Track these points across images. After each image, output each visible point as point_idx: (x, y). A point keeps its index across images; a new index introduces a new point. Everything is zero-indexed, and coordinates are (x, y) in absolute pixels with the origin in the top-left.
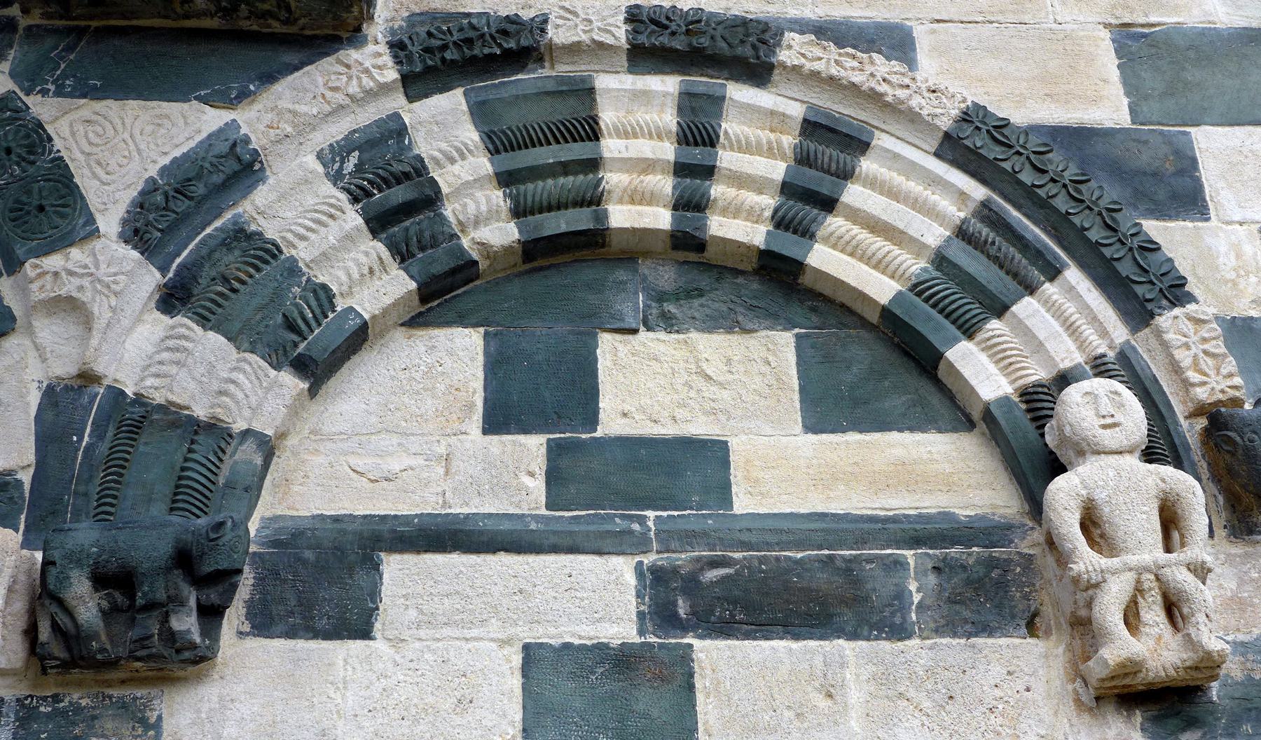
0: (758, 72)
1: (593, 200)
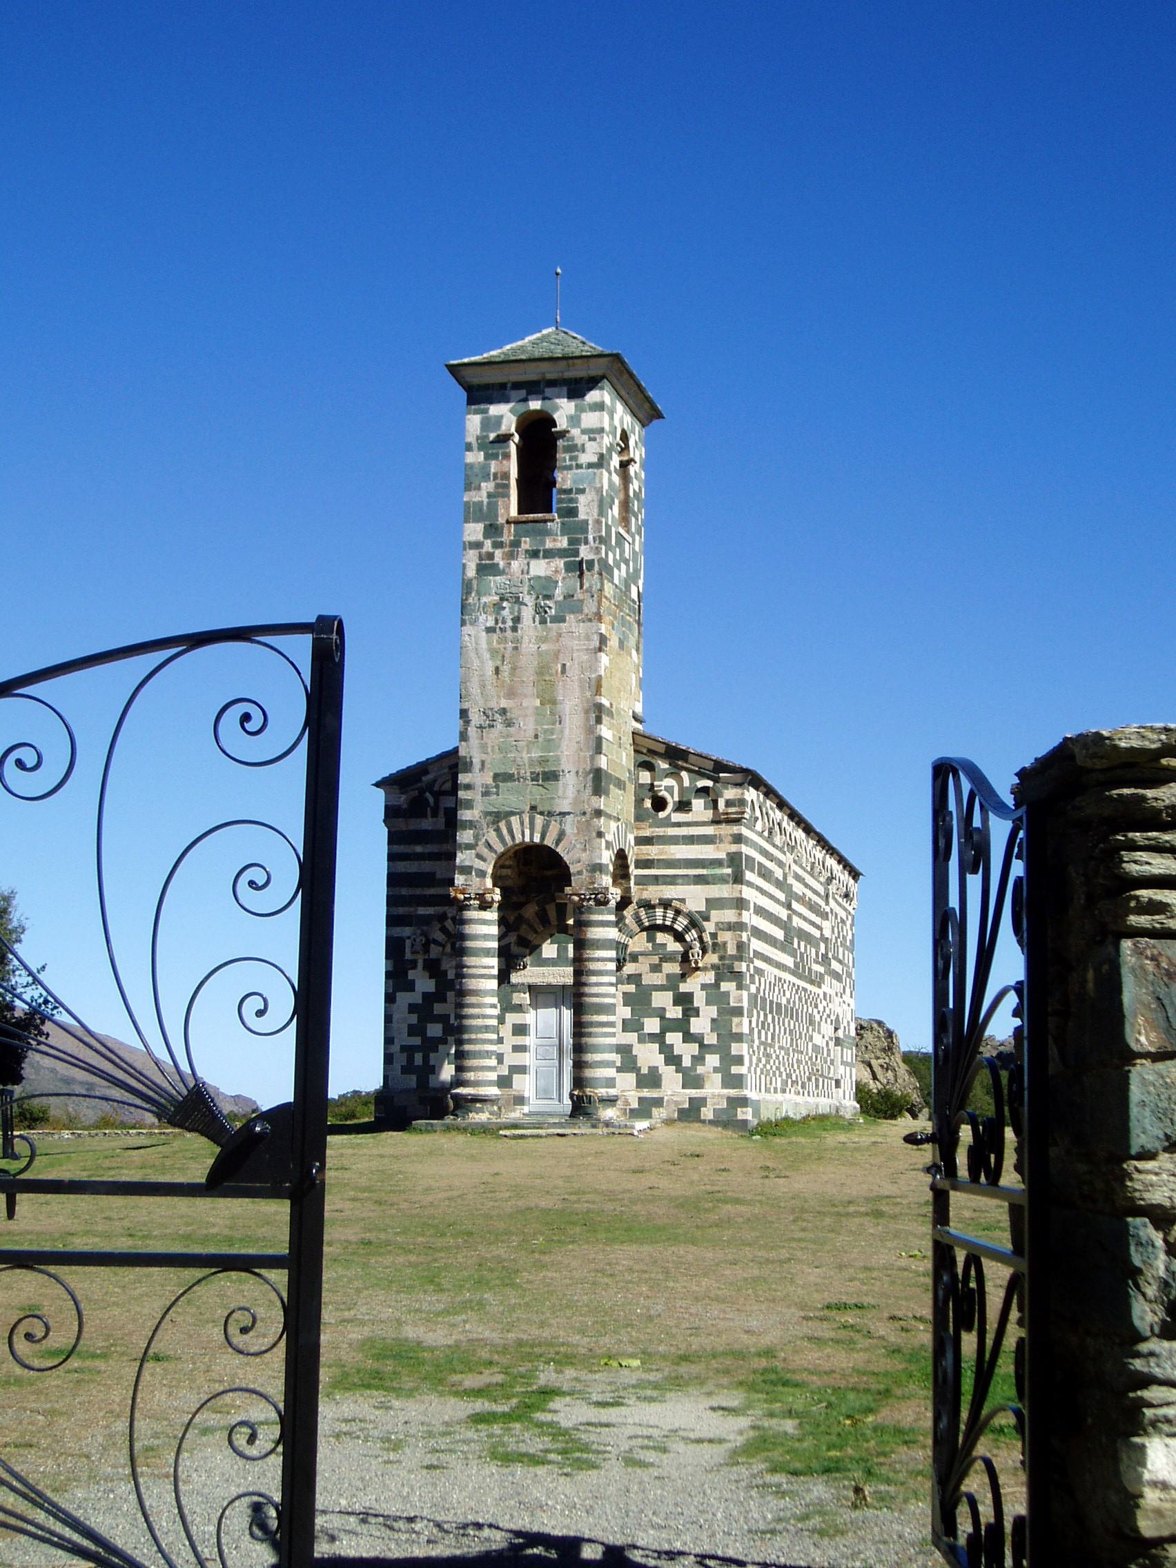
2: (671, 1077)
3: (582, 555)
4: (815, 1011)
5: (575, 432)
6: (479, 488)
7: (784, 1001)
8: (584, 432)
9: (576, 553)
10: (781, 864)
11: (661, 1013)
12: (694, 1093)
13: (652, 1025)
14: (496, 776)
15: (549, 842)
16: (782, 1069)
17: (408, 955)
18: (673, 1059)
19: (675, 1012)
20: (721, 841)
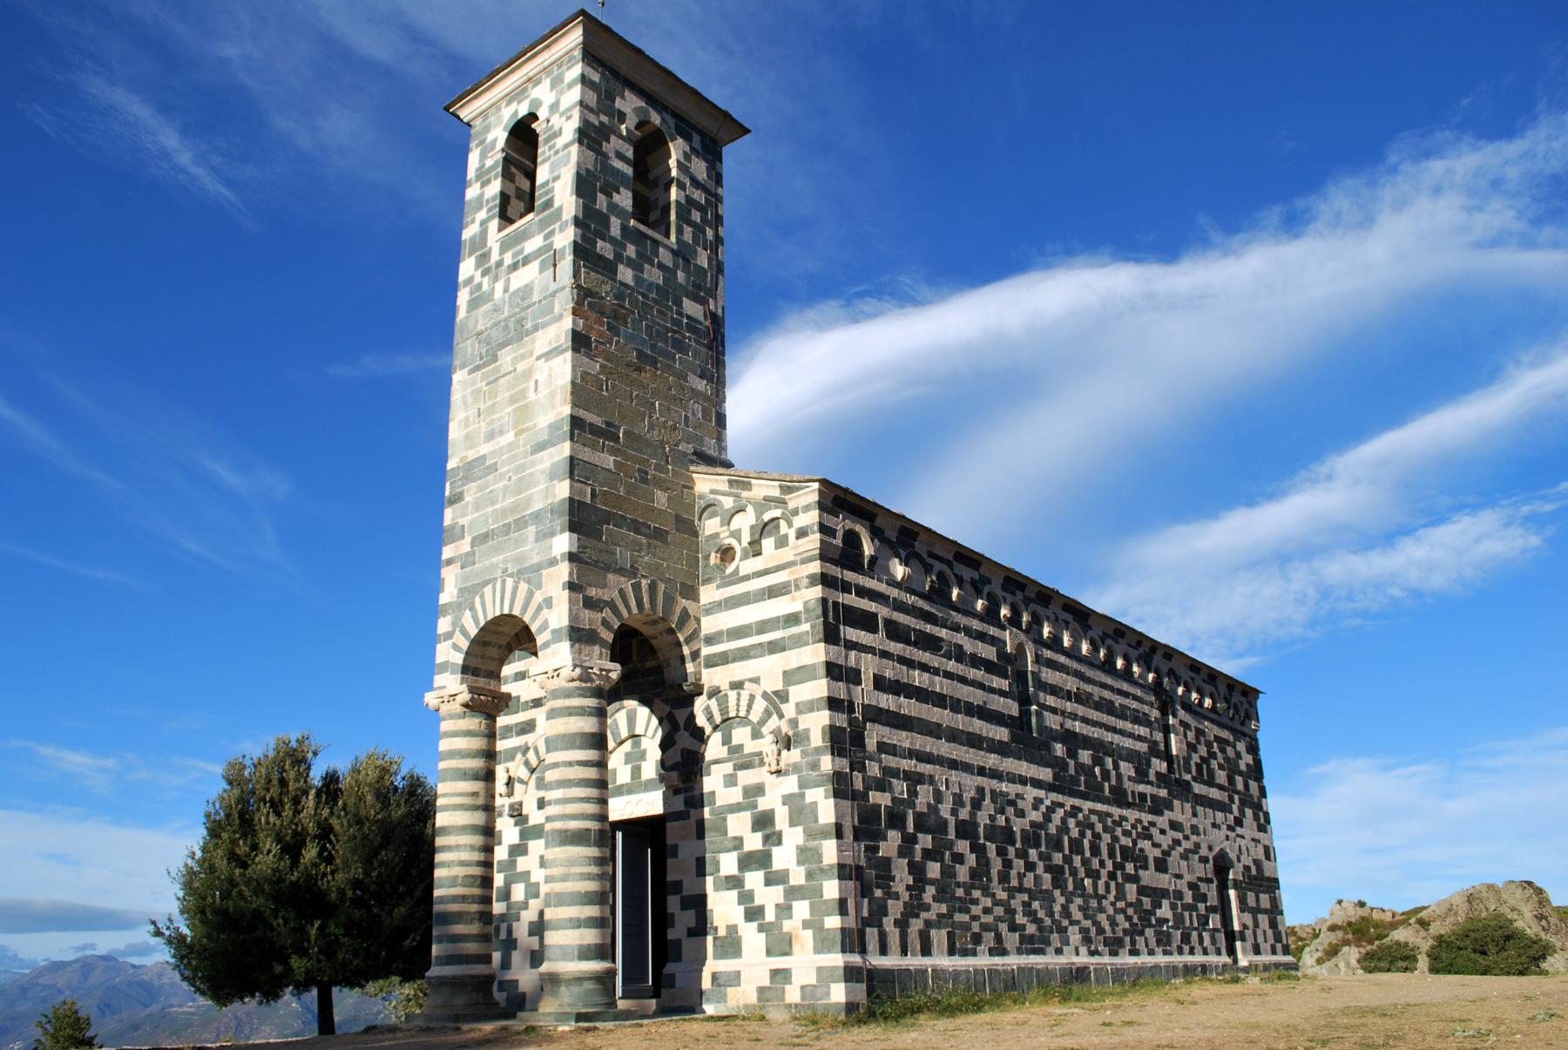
4: (1145, 844)
7: (1018, 825)
10: (982, 637)
11: (738, 843)
12: (780, 962)
16: (1020, 919)
18: (754, 913)
19: (754, 842)
20: (797, 588)
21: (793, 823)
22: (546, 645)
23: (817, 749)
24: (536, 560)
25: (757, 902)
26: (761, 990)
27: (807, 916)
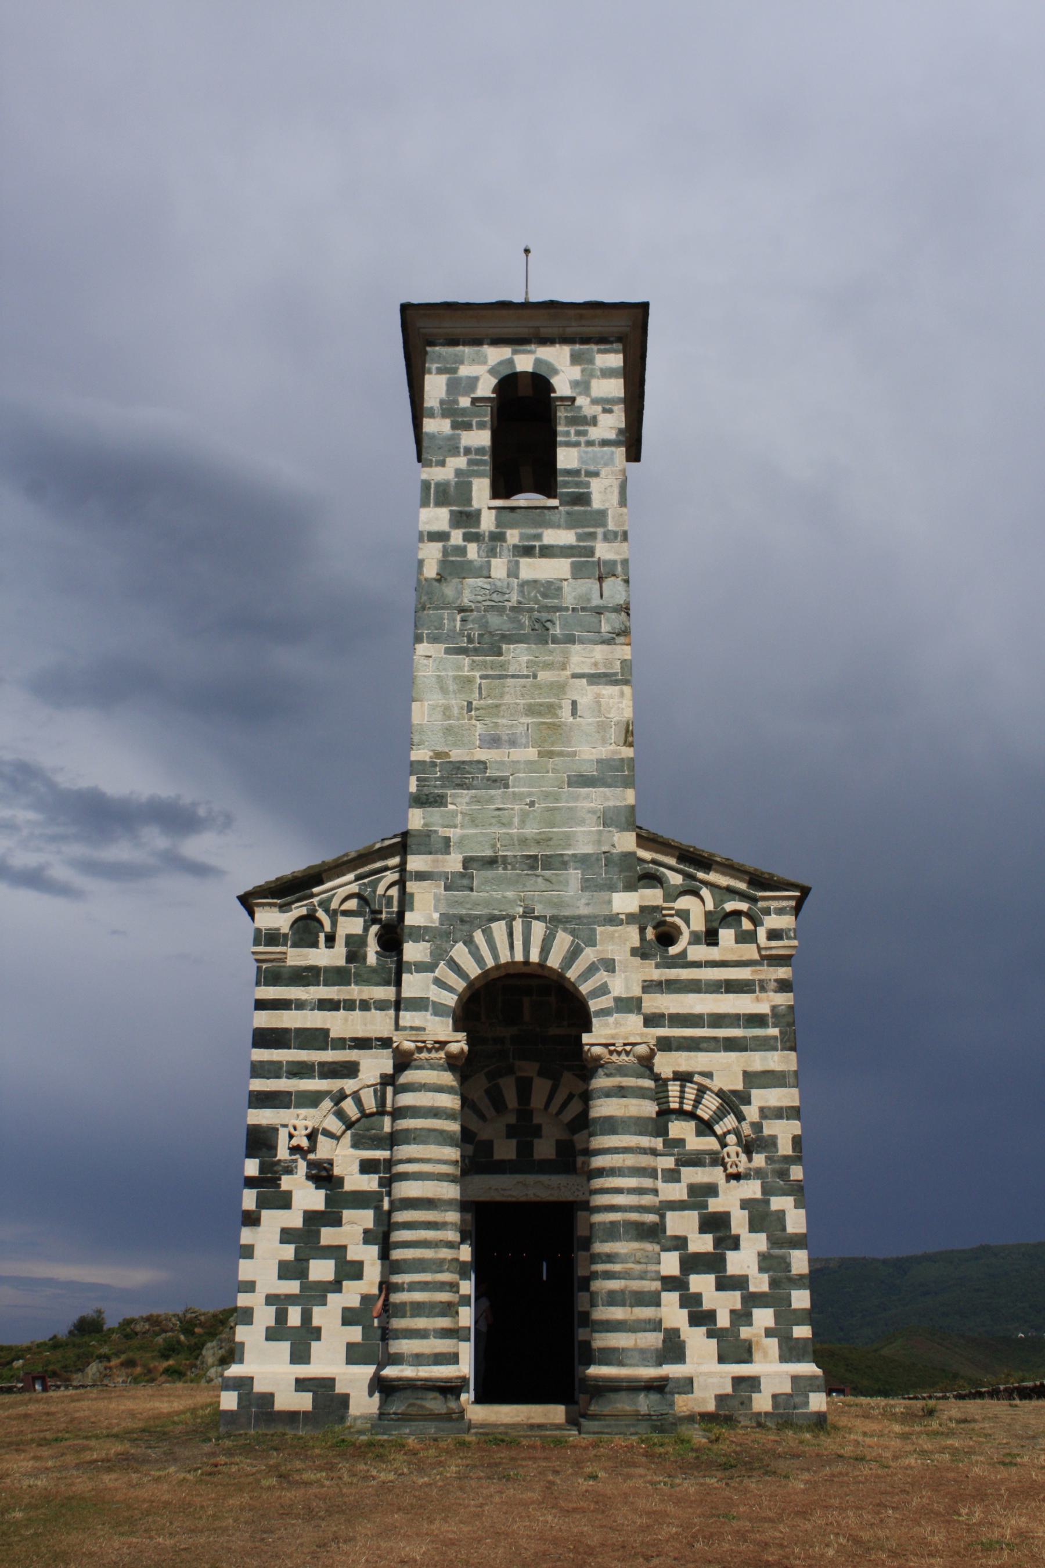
0: (691, 1082)
1: (668, 1102)
2: (699, 1345)
3: (598, 554)
5: (581, 401)
6: (442, 464)
8: (595, 402)
9: (591, 552)
11: (680, 1243)
13: (670, 1264)
14: (467, 862)
15: (554, 962)
17: (283, 1153)
18: (701, 1317)
19: (702, 1244)
20: (763, 989)
21: (753, 1229)
22: (605, 1012)
23: (786, 1159)
24: (584, 911)
25: (707, 1305)
26: (720, 1399)
27: (771, 1323)
